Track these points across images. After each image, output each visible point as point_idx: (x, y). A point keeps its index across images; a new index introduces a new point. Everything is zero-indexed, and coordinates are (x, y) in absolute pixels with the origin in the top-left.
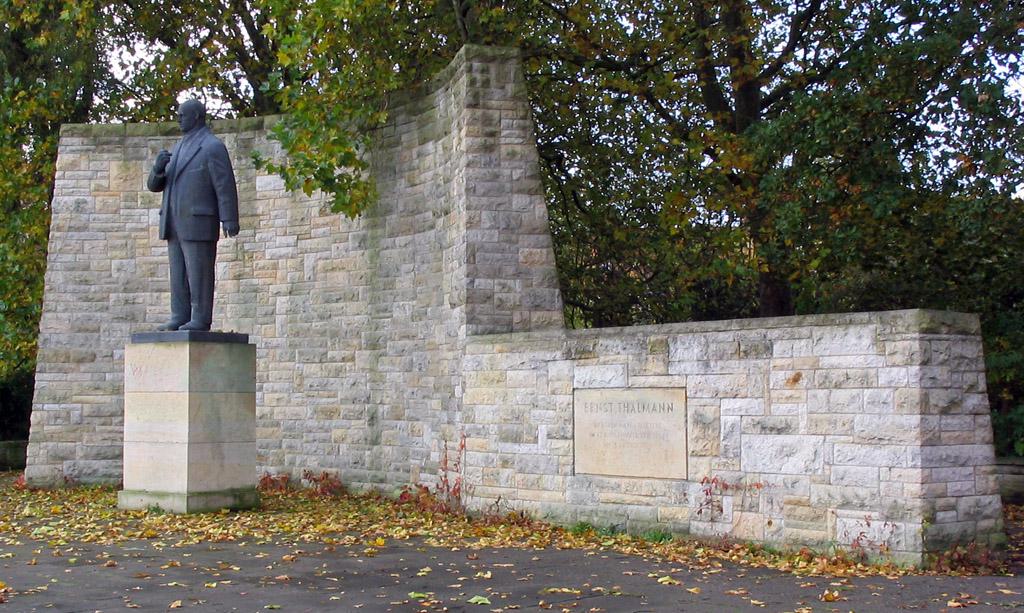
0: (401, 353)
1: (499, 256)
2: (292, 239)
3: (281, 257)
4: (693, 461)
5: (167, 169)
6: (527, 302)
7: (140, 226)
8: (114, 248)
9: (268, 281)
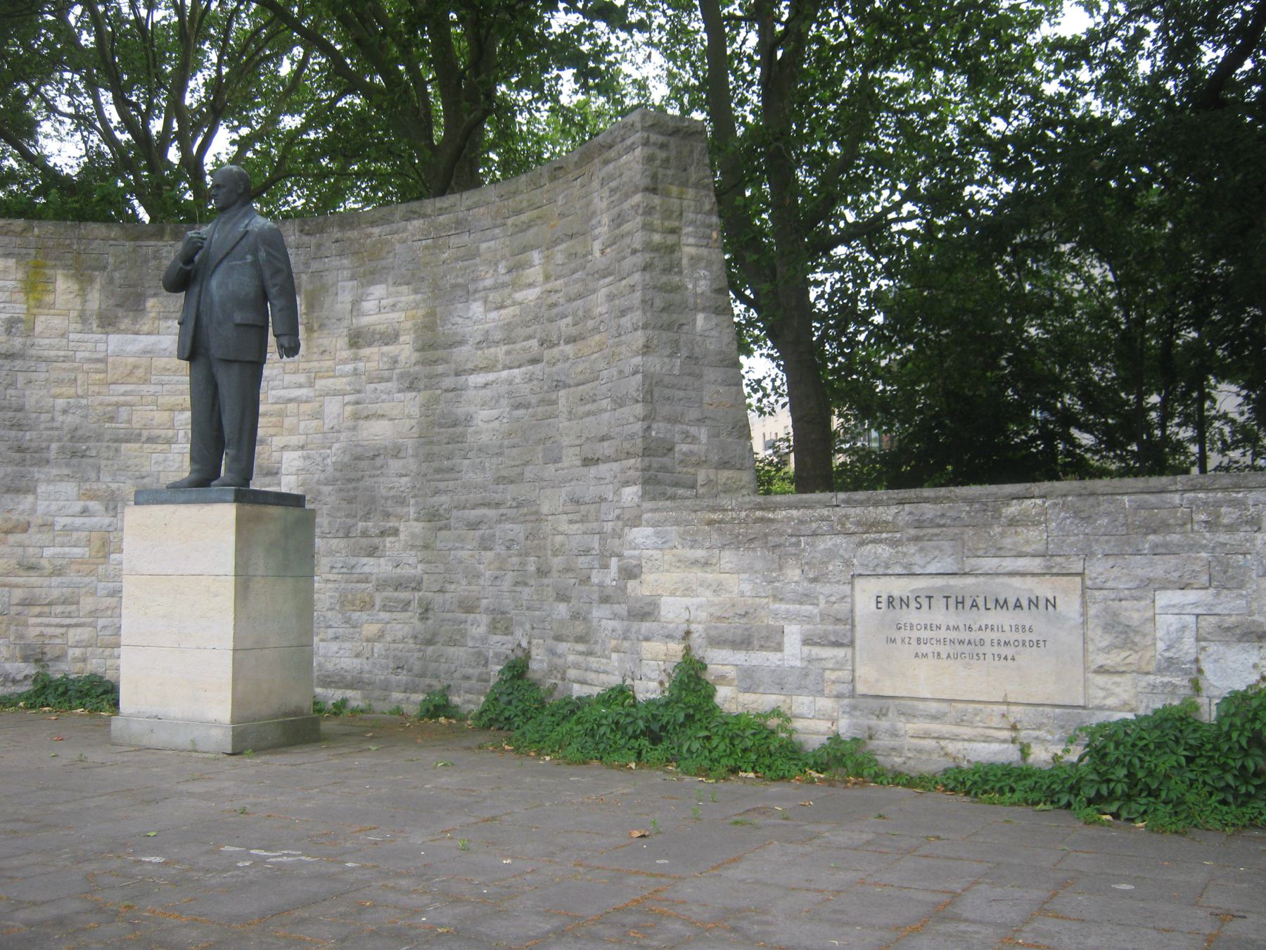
0: (473, 526)
1: (681, 394)
2: (302, 378)
3: (290, 400)
4: (1101, 680)
5: (197, 257)
6: (715, 458)
7: (95, 356)
8: (59, 382)
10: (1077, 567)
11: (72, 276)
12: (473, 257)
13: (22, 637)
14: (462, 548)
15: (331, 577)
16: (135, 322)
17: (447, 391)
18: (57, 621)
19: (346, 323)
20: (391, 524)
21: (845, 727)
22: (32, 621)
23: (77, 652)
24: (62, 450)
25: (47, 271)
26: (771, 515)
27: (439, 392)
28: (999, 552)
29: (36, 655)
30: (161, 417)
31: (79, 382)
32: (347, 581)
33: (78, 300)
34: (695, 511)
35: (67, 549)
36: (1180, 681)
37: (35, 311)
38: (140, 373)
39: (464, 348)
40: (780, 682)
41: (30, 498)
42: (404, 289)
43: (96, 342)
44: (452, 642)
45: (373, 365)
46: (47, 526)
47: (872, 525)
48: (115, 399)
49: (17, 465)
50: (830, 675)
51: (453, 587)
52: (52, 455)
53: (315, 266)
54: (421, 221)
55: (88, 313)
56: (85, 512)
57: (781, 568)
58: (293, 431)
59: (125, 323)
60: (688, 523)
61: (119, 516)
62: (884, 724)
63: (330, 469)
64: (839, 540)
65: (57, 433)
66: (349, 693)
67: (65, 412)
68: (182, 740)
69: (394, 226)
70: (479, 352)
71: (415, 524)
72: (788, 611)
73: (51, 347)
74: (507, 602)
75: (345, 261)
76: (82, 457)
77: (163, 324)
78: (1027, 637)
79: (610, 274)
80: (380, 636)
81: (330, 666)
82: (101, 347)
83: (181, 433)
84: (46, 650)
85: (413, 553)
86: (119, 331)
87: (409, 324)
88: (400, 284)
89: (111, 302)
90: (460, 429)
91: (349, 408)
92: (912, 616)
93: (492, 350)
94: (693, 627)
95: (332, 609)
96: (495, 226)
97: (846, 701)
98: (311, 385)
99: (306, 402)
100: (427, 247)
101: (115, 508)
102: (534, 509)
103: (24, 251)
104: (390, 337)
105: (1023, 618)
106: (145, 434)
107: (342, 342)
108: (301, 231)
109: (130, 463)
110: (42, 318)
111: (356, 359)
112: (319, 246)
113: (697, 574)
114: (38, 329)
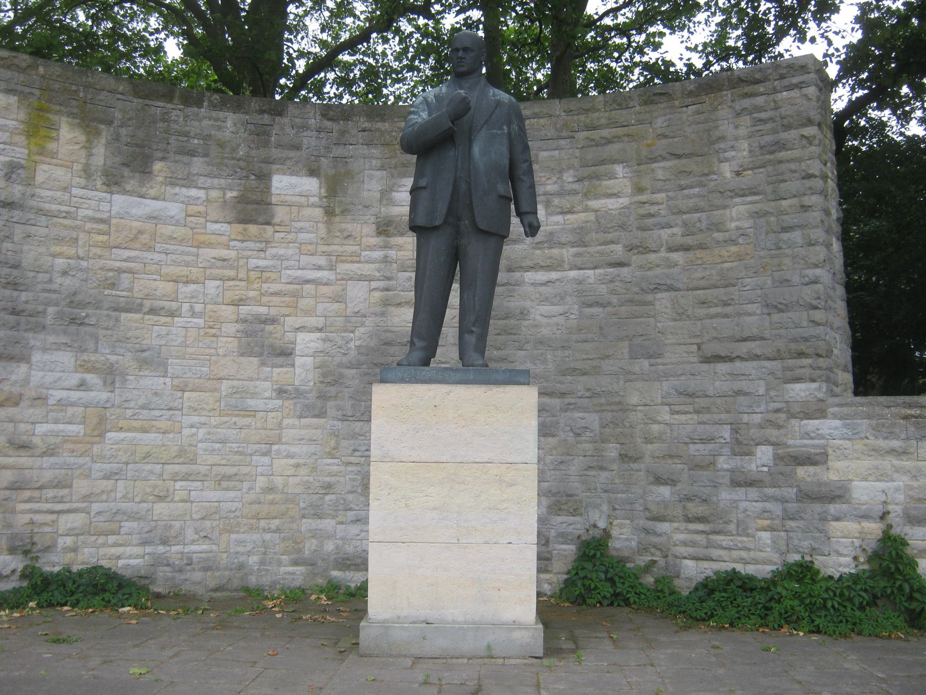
2: (322, 261)
3: (308, 282)
7: (98, 215)
8: (59, 240)
9: (286, 311)
11: (79, 125)
13: (9, 526)
15: (352, 459)
16: (142, 184)
18: (49, 506)
19: (374, 210)
22: (21, 507)
23: (69, 541)
24: (60, 316)
25: (50, 116)
29: (24, 547)
30: (164, 287)
31: (81, 243)
33: (83, 153)
34: (888, 407)
35: (61, 427)
37: (37, 158)
38: (145, 238)
41: (24, 367)
43: (100, 200)
46: (40, 399)
48: (118, 264)
49: (11, 328)
52: (49, 320)
53: (338, 151)
55: (93, 168)
56: (82, 385)
58: (308, 313)
59: (131, 185)
60: (882, 417)
61: (117, 391)
63: (353, 353)
65: (54, 296)
67: (65, 273)
70: (538, 252)
73: (53, 200)
74: (575, 484)
75: (375, 152)
76: (81, 324)
77: (171, 190)
79: (755, 194)
82: (105, 206)
83: (186, 307)
84: (36, 539)
86: (125, 192)
89: (118, 160)
90: (512, 322)
91: (377, 294)
93: (555, 251)
94: (890, 507)
95: (352, 492)
98: (332, 268)
99: (325, 284)
101: (113, 382)
102: (617, 399)
103: (27, 90)
106: (148, 304)
107: (370, 229)
109: (130, 334)
110: (45, 167)
111: (386, 246)
112: (343, 133)
113: (888, 463)
114: (40, 178)
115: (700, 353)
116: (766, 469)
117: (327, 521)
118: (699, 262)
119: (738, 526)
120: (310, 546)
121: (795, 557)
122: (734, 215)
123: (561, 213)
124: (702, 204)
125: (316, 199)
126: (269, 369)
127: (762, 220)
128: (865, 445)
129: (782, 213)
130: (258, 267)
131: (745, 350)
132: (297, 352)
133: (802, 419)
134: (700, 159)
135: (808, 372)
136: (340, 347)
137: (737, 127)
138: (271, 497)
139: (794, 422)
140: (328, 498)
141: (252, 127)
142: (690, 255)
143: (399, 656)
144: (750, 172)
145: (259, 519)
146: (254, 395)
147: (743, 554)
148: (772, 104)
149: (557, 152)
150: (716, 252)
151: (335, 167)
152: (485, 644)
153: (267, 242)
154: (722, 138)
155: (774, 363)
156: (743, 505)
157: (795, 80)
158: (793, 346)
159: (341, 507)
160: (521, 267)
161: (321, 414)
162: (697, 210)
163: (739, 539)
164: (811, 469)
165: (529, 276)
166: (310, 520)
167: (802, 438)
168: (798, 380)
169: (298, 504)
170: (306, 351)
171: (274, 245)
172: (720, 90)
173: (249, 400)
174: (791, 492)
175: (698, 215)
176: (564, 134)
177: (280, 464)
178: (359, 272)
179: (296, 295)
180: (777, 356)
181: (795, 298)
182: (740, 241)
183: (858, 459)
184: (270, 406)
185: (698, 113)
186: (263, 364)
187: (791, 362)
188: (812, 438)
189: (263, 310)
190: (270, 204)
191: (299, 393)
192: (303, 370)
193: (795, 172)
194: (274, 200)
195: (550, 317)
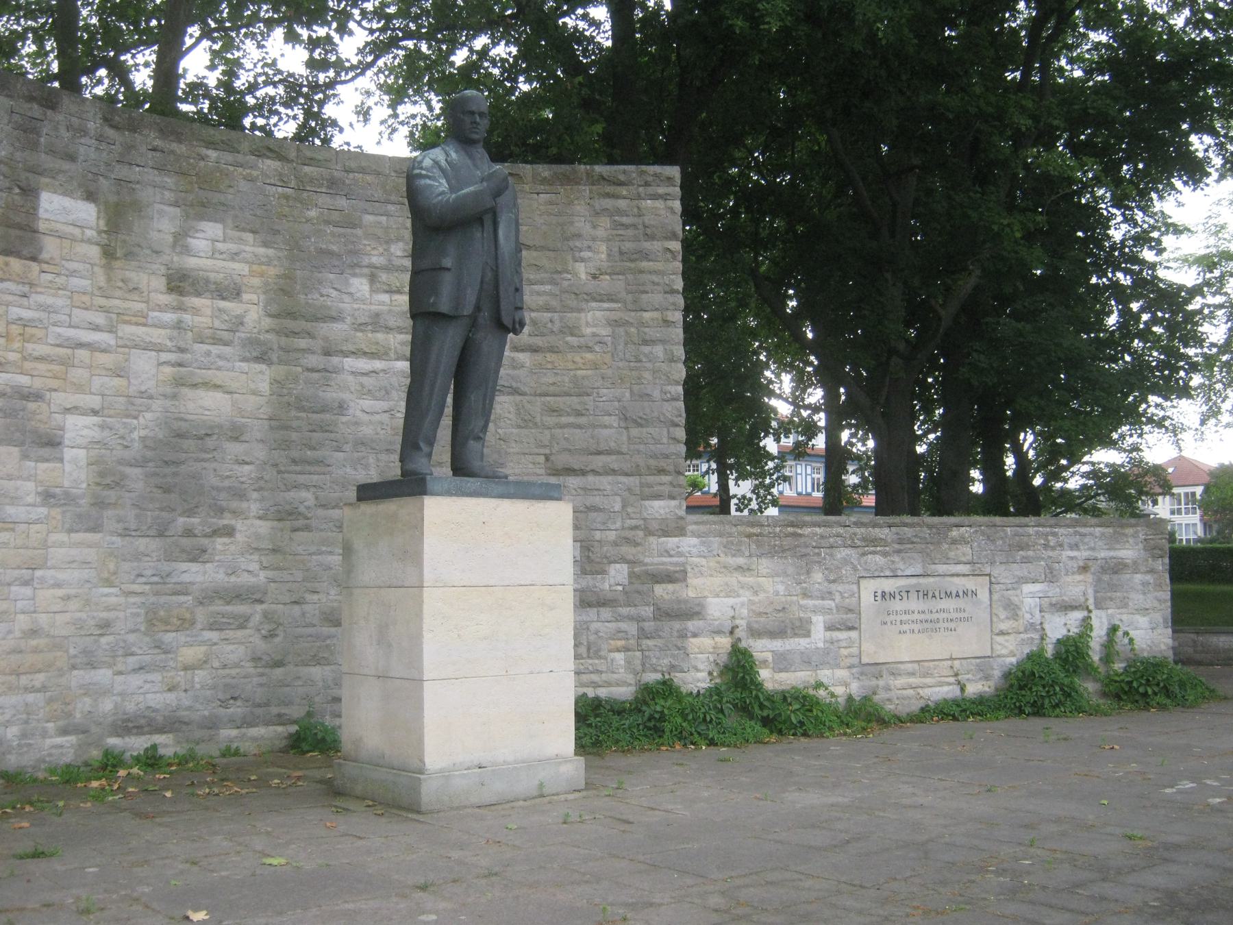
2: (100, 319)
3: (81, 345)
4: (999, 639)
9: (55, 384)
10: (987, 570)
12: (354, 226)
14: (331, 553)
15: (137, 588)
17: (308, 370)
19: (165, 258)
20: (226, 522)
21: (856, 689)
26: (799, 531)
27: (299, 369)
28: (946, 561)
32: (157, 594)
36: (1036, 636)
39: (337, 326)
40: (807, 660)
42: (249, 237)
44: (317, 661)
45: (203, 321)
47: (874, 542)
50: (844, 652)
51: (315, 597)
53: (122, 172)
54: (278, 163)
57: (808, 572)
58: (79, 388)
60: (730, 535)
62: (881, 683)
64: (848, 551)
66: (159, 739)
68: (525, 785)
69: (240, 158)
70: (359, 334)
71: (258, 522)
72: (815, 606)
75: (169, 181)
78: (962, 615)
79: (612, 301)
80: (203, 663)
81: (130, 707)
85: (255, 557)
87: (256, 281)
88: (244, 230)
90: (327, 416)
91: (168, 370)
92: (897, 605)
93: (380, 336)
94: (738, 622)
95: (133, 631)
96: (388, 202)
97: (854, 670)
98: (111, 331)
99: (104, 351)
100: (287, 197)
104: (231, 291)
105: (960, 603)
107: (159, 283)
108: (105, 119)
111: (180, 308)
113: (734, 579)
115: (549, 465)
116: (620, 588)
117: (102, 671)
118: (549, 366)
119: (589, 649)
120: (83, 705)
121: (652, 677)
122: (590, 320)
123: (387, 292)
124: (554, 303)
125: (94, 233)
126: (32, 464)
127: (621, 329)
128: (718, 562)
129: (642, 324)
130: (21, 319)
131: (600, 464)
132: (67, 442)
133: (659, 537)
134: (551, 254)
135: (666, 489)
136: (122, 438)
137: (594, 227)
138: (34, 643)
139: (652, 539)
140: (103, 640)
141: (16, 118)
142: (539, 357)
143: (458, 808)
144: (607, 277)
145: (18, 675)
146: (15, 500)
147: (595, 677)
148: (635, 210)
149: (384, 218)
150: (569, 356)
151: (118, 193)
152: (537, 782)
153: (31, 285)
154: (578, 236)
155: (631, 479)
156: (594, 626)
157: (661, 190)
158: (652, 462)
159: (120, 653)
160: (342, 351)
161: (95, 529)
162: (547, 309)
163: (590, 661)
164: (670, 587)
165: (349, 362)
166: (82, 672)
167: (661, 556)
168: (658, 497)
169: (67, 651)
170: (79, 441)
171: (39, 290)
172: (578, 183)
173: (7, 507)
174: (648, 611)
175: (549, 315)
176: (393, 198)
177: (46, 595)
178: (148, 339)
179: (66, 363)
180: (636, 472)
181: (656, 414)
182: (597, 348)
183: (711, 576)
184: (33, 516)
185: (551, 203)
186: (25, 457)
187: (651, 479)
188: (671, 556)
189: (24, 380)
190: (36, 231)
191: (69, 499)
192: (73, 468)
193: (658, 284)
194: (42, 226)
195: (372, 414)
